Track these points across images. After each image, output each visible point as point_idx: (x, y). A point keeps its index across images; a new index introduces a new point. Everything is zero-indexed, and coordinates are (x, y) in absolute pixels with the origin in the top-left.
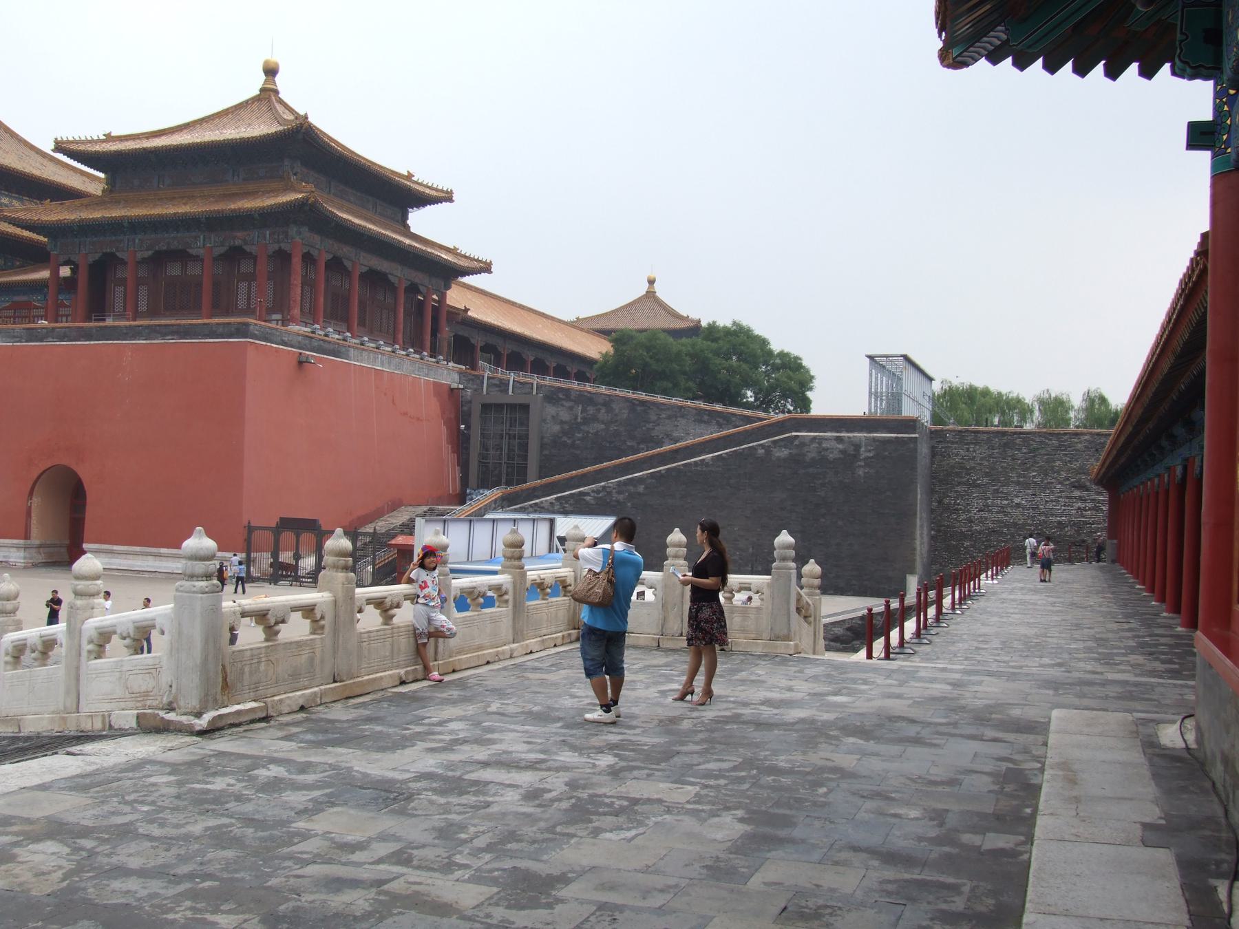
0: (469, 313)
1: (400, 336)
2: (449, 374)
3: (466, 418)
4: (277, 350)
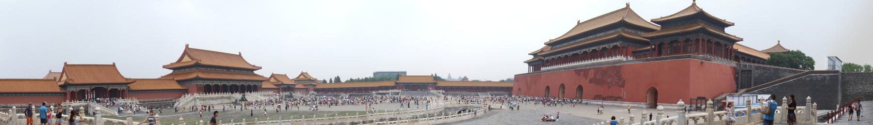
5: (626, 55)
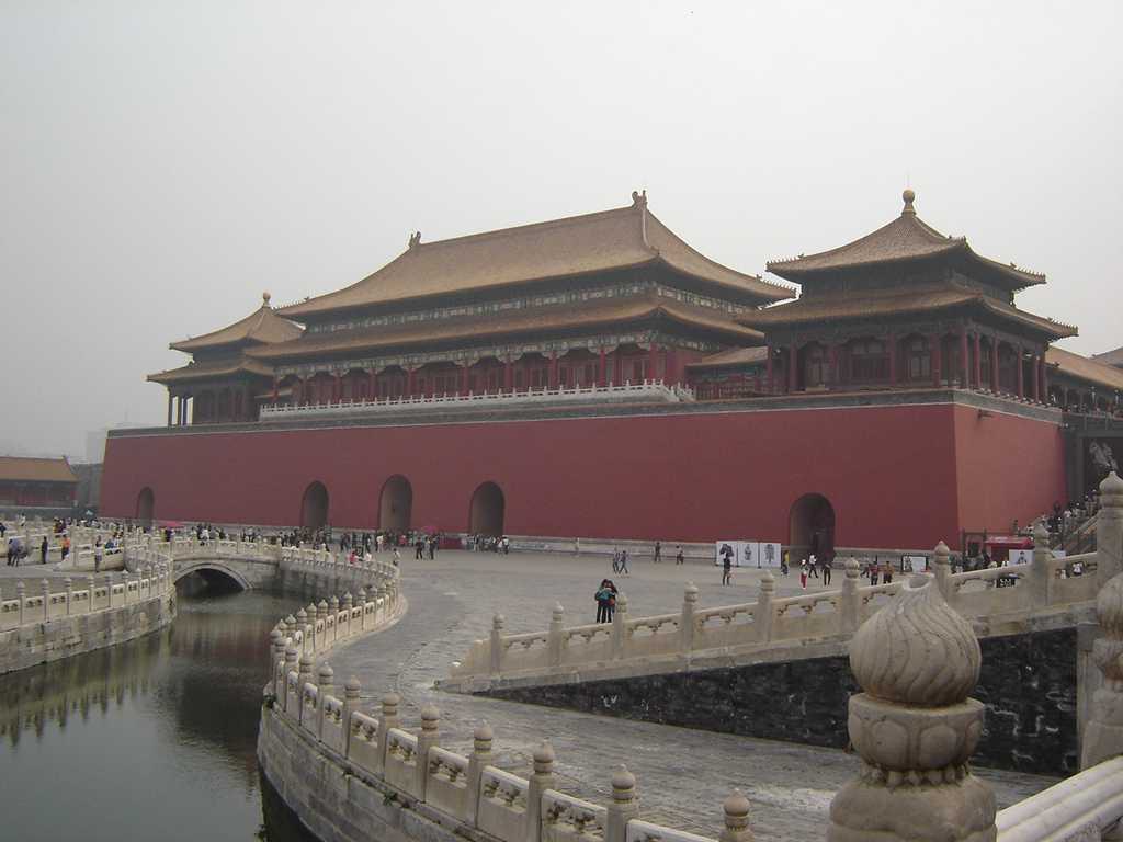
5: (669, 383)
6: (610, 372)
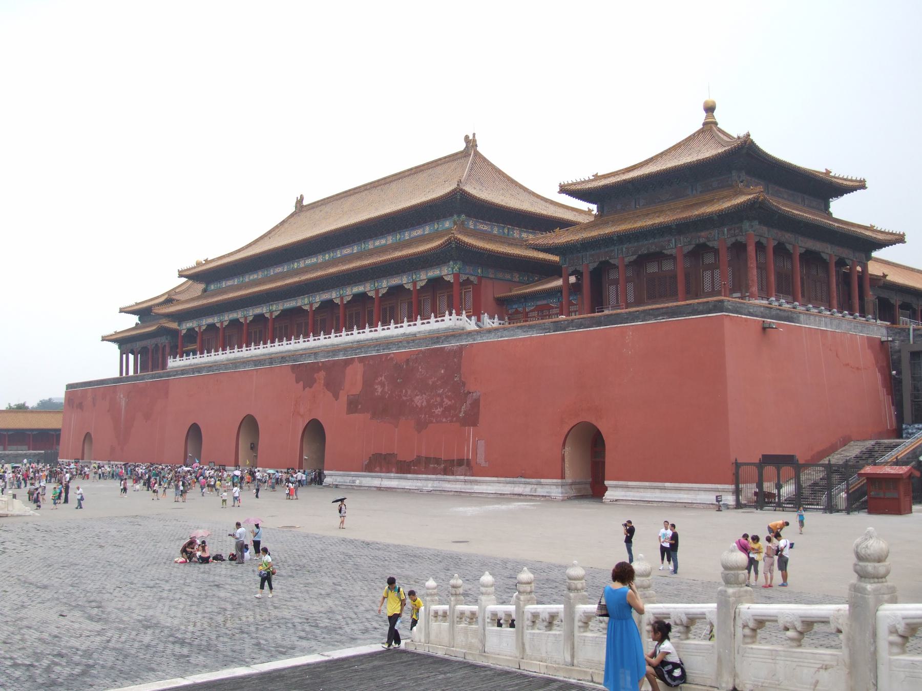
0: (888, 278)
1: (835, 302)
2: (878, 330)
3: (896, 365)
4: (746, 320)
5: (476, 312)
6: (428, 307)
